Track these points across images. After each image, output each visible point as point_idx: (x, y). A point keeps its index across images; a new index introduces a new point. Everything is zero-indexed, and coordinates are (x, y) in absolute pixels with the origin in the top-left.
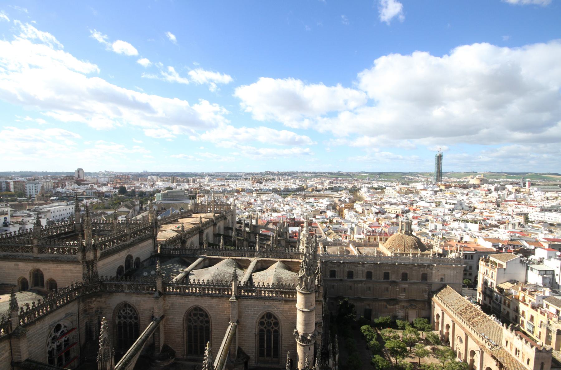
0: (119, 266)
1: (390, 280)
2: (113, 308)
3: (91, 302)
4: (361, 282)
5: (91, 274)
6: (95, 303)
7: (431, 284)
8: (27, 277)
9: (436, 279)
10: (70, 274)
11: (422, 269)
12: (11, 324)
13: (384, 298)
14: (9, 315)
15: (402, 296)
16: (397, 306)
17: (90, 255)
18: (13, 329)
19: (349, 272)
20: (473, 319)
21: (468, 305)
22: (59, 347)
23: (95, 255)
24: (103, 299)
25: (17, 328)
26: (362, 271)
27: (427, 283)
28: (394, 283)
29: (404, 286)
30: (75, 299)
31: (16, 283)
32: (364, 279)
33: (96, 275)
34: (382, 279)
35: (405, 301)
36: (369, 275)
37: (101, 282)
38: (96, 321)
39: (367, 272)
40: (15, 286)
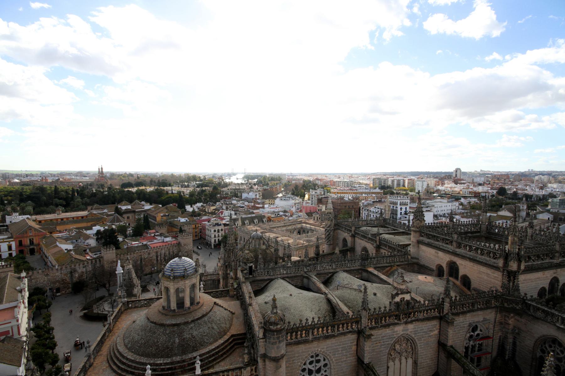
0: (541, 286)
2: (537, 336)
3: (508, 317)
5: (511, 287)
6: (512, 320)
8: (444, 266)
10: (486, 278)
12: (443, 308)
14: (443, 299)
17: (513, 266)
18: (445, 313)
22: (473, 347)
23: (519, 266)
24: (523, 320)
25: (447, 314)
30: (494, 308)
31: (434, 268)
33: (517, 289)
37: (524, 300)
38: (511, 341)
40: (433, 270)
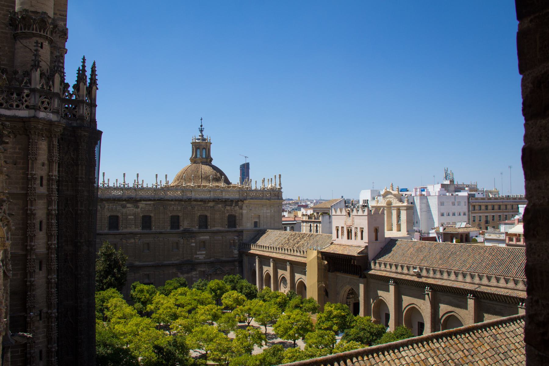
1: (181, 229)
4: (133, 234)
7: (241, 233)
9: (247, 225)
11: (228, 208)
13: (174, 261)
15: (201, 256)
16: (194, 273)
19: (111, 217)
20: (297, 244)
21: (291, 235)
26: (134, 214)
27: (235, 231)
28: (188, 234)
29: (202, 237)
32: (139, 230)
34: (168, 229)
35: (205, 263)
36: (146, 222)
39: (144, 217)
